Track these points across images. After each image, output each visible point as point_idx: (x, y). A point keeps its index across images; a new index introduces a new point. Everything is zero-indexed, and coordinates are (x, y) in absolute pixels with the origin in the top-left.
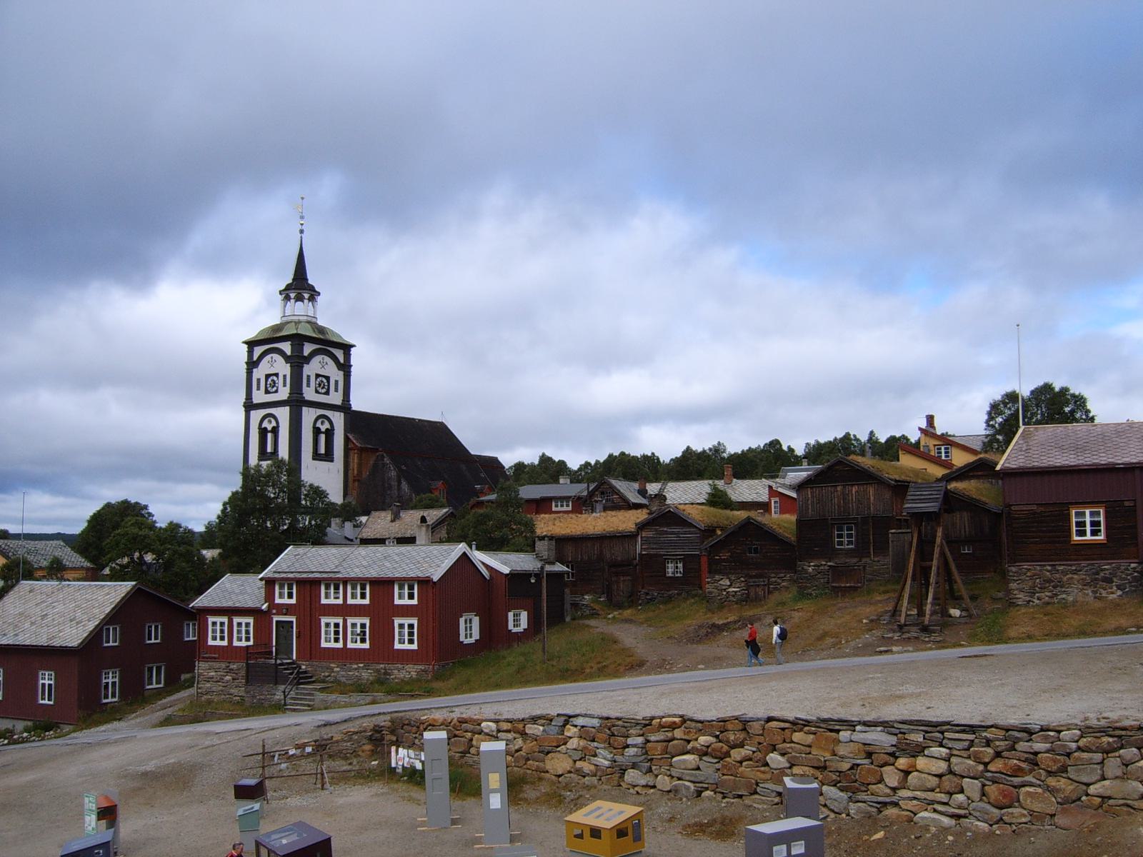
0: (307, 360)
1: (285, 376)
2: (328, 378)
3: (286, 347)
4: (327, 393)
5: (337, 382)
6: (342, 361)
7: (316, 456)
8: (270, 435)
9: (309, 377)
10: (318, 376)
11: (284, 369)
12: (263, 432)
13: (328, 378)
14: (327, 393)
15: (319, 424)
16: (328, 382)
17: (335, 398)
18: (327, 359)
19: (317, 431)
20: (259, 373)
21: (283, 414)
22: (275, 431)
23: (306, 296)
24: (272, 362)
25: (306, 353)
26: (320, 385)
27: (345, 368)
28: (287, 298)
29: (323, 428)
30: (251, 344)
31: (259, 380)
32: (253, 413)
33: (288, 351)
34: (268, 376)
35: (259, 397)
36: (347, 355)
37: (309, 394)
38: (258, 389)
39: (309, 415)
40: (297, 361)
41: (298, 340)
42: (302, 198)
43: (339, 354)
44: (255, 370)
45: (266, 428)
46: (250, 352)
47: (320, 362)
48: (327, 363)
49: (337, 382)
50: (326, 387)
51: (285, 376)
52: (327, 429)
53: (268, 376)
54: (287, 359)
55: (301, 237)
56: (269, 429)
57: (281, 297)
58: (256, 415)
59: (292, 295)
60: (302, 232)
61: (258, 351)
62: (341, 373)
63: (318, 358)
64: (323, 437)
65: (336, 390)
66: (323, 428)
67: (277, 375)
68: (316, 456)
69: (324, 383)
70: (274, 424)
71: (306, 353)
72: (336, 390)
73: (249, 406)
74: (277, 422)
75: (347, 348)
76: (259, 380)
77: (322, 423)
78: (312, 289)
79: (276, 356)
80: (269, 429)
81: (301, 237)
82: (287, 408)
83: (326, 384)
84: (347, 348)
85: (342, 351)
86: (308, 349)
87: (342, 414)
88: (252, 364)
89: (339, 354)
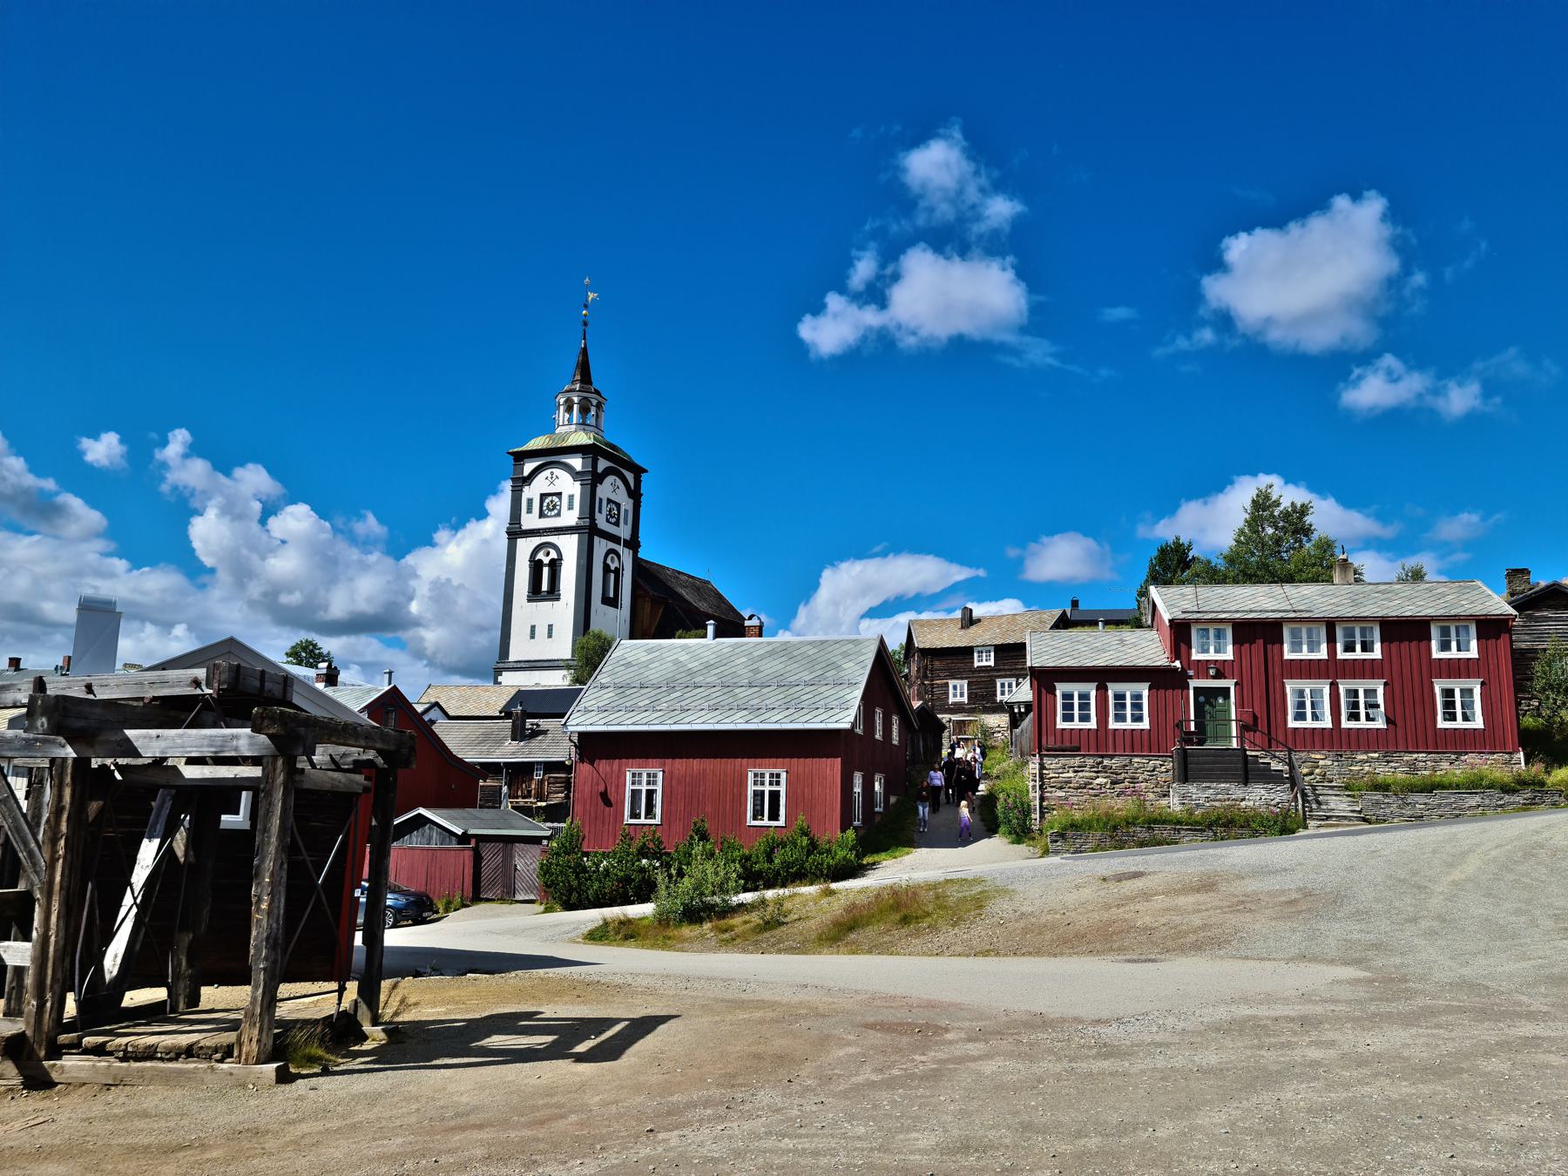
0: (528, 480)
4: (558, 514)
5: (571, 497)
7: (535, 593)
9: (530, 501)
10: (543, 496)
14: (558, 514)
18: (557, 472)
19: (536, 567)
29: (546, 560)
37: (529, 521)
39: (525, 546)
49: (571, 497)
52: (553, 561)
63: (547, 473)
64: (546, 570)
65: (570, 507)
66: (546, 560)
69: (549, 503)
72: (570, 507)
89: (577, 462)
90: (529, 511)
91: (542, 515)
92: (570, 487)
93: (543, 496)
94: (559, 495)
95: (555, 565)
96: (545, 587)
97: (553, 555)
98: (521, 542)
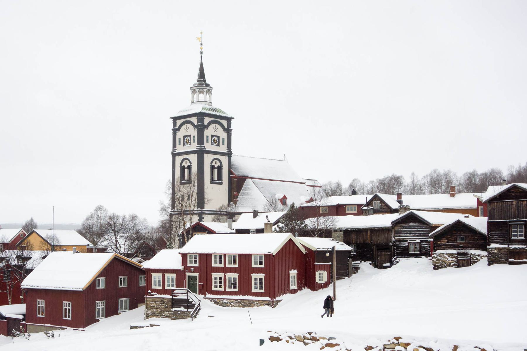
0: (207, 127)
1: (194, 137)
2: (218, 137)
3: (194, 120)
4: (219, 145)
5: (223, 139)
6: (226, 128)
7: (213, 181)
8: (186, 170)
10: (212, 136)
11: (193, 132)
12: (183, 169)
13: (218, 137)
15: (214, 164)
17: (223, 149)
19: (213, 168)
20: (180, 135)
21: (194, 158)
22: (189, 167)
23: (205, 90)
24: (187, 128)
25: (206, 123)
26: (214, 140)
27: (228, 130)
28: (194, 91)
29: (216, 166)
30: (175, 119)
31: (180, 139)
32: (177, 158)
33: (196, 123)
34: (185, 137)
35: (180, 149)
36: (229, 125)
37: (208, 146)
38: (180, 144)
39: (208, 159)
40: (201, 129)
41: (201, 116)
42: (201, 33)
43: (225, 123)
44: (177, 134)
45: (184, 166)
46: (175, 125)
49: (223, 139)
51: (194, 137)
52: (218, 166)
53: (185, 137)
54: (195, 127)
56: (186, 167)
57: (190, 91)
58: (179, 159)
59: (197, 90)
60: (201, 53)
61: (179, 122)
62: (226, 134)
63: (213, 125)
64: (216, 170)
65: (223, 144)
66: (216, 166)
67: (190, 136)
68: (213, 181)
69: (216, 140)
70: (189, 164)
71: (206, 123)
72: (223, 144)
73: (175, 155)
74: (191, 163)
75: (229, 120)
76: (180, 139)
78: (208, 85)
79: (189, 125)
80: (186, 167)
82: (196, 155)
84: (229, 120)
86: (207, 120)
87: (227, 157)
88: (176, 130)
89: (225, 123)
91: (212, 144)
92: (224, 136)
95: (220, 169)
96: (216, 178)
98: (206, 155)
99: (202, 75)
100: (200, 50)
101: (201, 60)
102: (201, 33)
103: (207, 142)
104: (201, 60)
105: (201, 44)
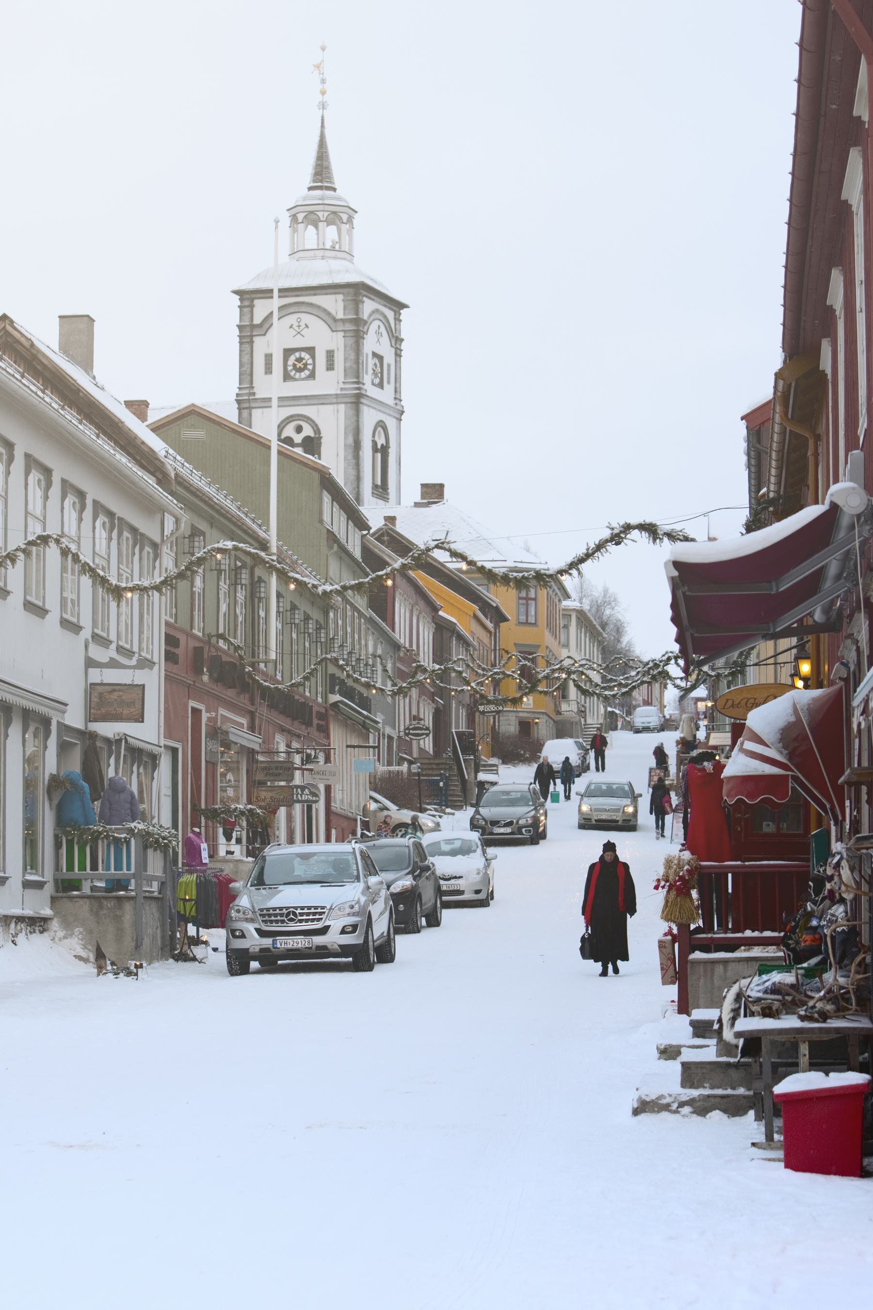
2: (311, 351)
4: (312, 376)
5: (330, 355)
6: (340, 315)
9: (269, 358)
10: (288, 352)
15: (289, 431)
16: (313, 357)
18: (306, 318)
29: (298, 438)
42: (323, 49)
47: (291, 327)
48: (307, 326)
49: (330, 355)
50: (310, 367)
52: (307, 439)
55: (323, 117)
60: (323, 106)
65: (330, 367)
72: (330, 367)
77: (299, 429)
81: (323, 117)
83: (310, 361)
85: (340, 297)
89: (335, 304)
90: (268, 370)
91: (287, 377)
93: (288, 352)
94: (311, 351)
97: (308, 431)
99: (322, 173)
100: (320, 98)
101: (323, 126)
102: (323, 49)
103: (268, 370)
104: (323, 126)
105: (323, 81)
